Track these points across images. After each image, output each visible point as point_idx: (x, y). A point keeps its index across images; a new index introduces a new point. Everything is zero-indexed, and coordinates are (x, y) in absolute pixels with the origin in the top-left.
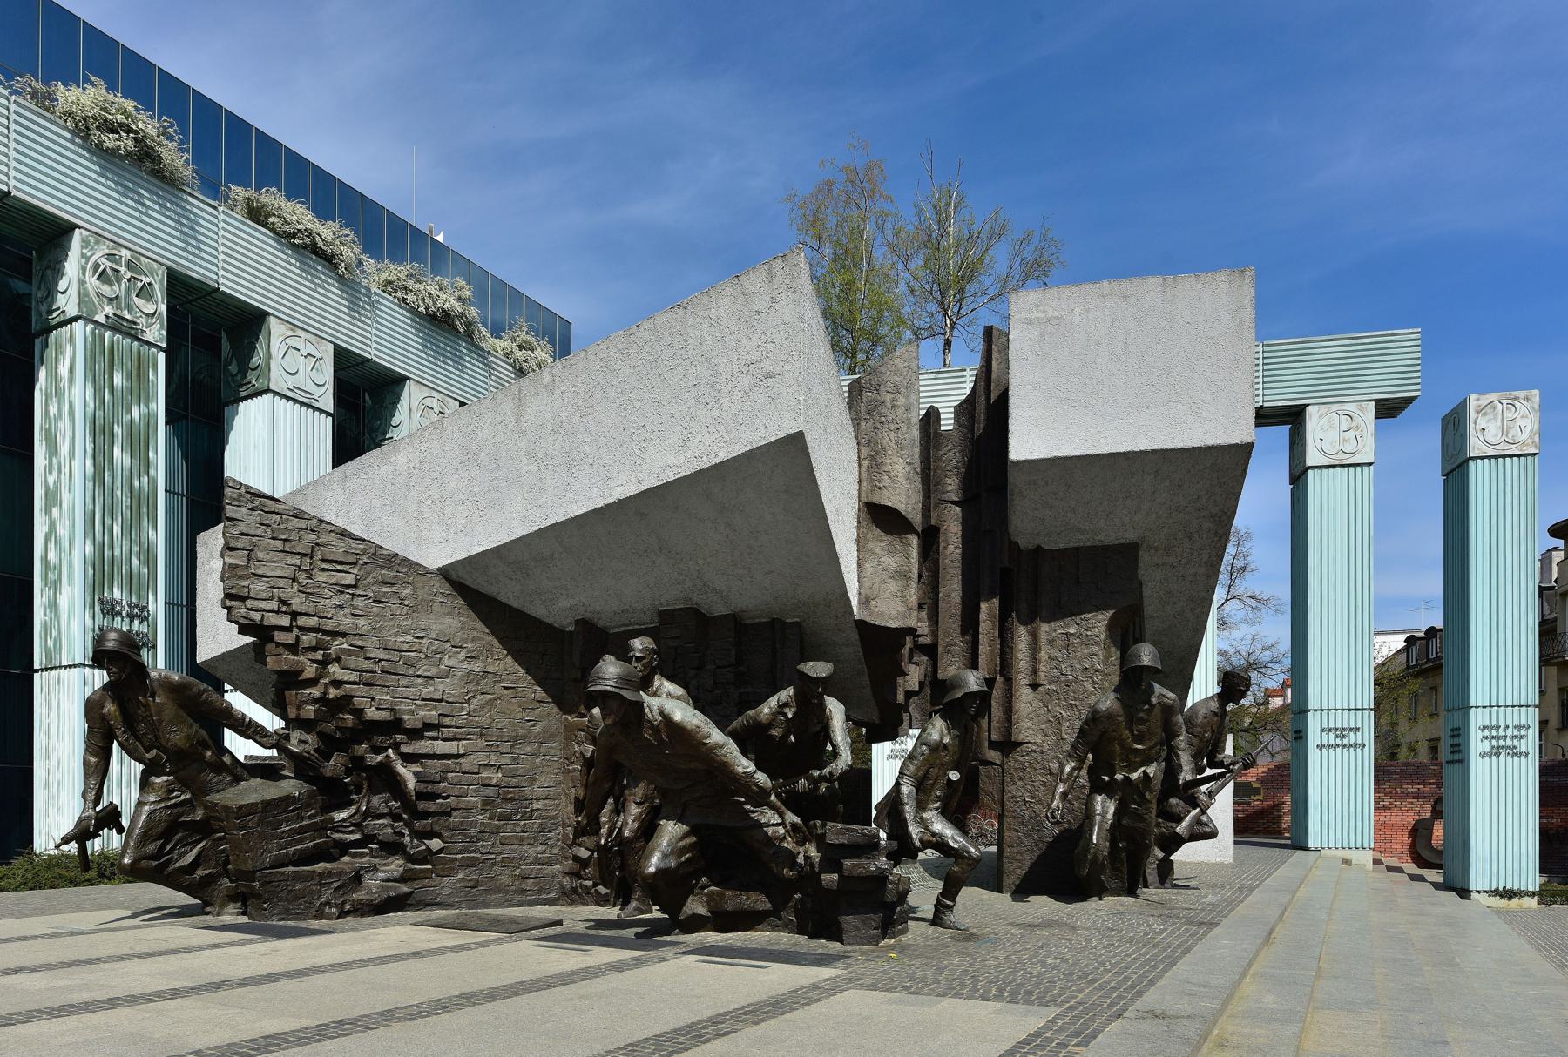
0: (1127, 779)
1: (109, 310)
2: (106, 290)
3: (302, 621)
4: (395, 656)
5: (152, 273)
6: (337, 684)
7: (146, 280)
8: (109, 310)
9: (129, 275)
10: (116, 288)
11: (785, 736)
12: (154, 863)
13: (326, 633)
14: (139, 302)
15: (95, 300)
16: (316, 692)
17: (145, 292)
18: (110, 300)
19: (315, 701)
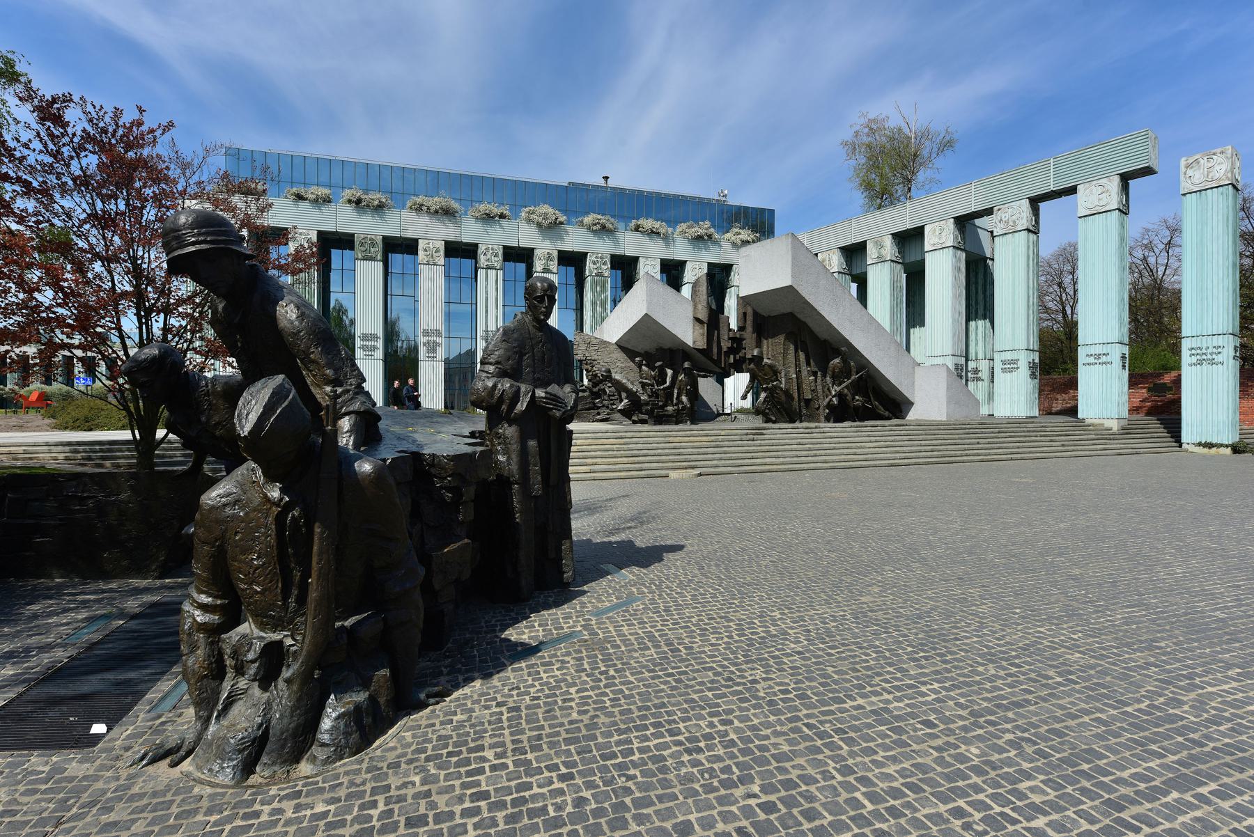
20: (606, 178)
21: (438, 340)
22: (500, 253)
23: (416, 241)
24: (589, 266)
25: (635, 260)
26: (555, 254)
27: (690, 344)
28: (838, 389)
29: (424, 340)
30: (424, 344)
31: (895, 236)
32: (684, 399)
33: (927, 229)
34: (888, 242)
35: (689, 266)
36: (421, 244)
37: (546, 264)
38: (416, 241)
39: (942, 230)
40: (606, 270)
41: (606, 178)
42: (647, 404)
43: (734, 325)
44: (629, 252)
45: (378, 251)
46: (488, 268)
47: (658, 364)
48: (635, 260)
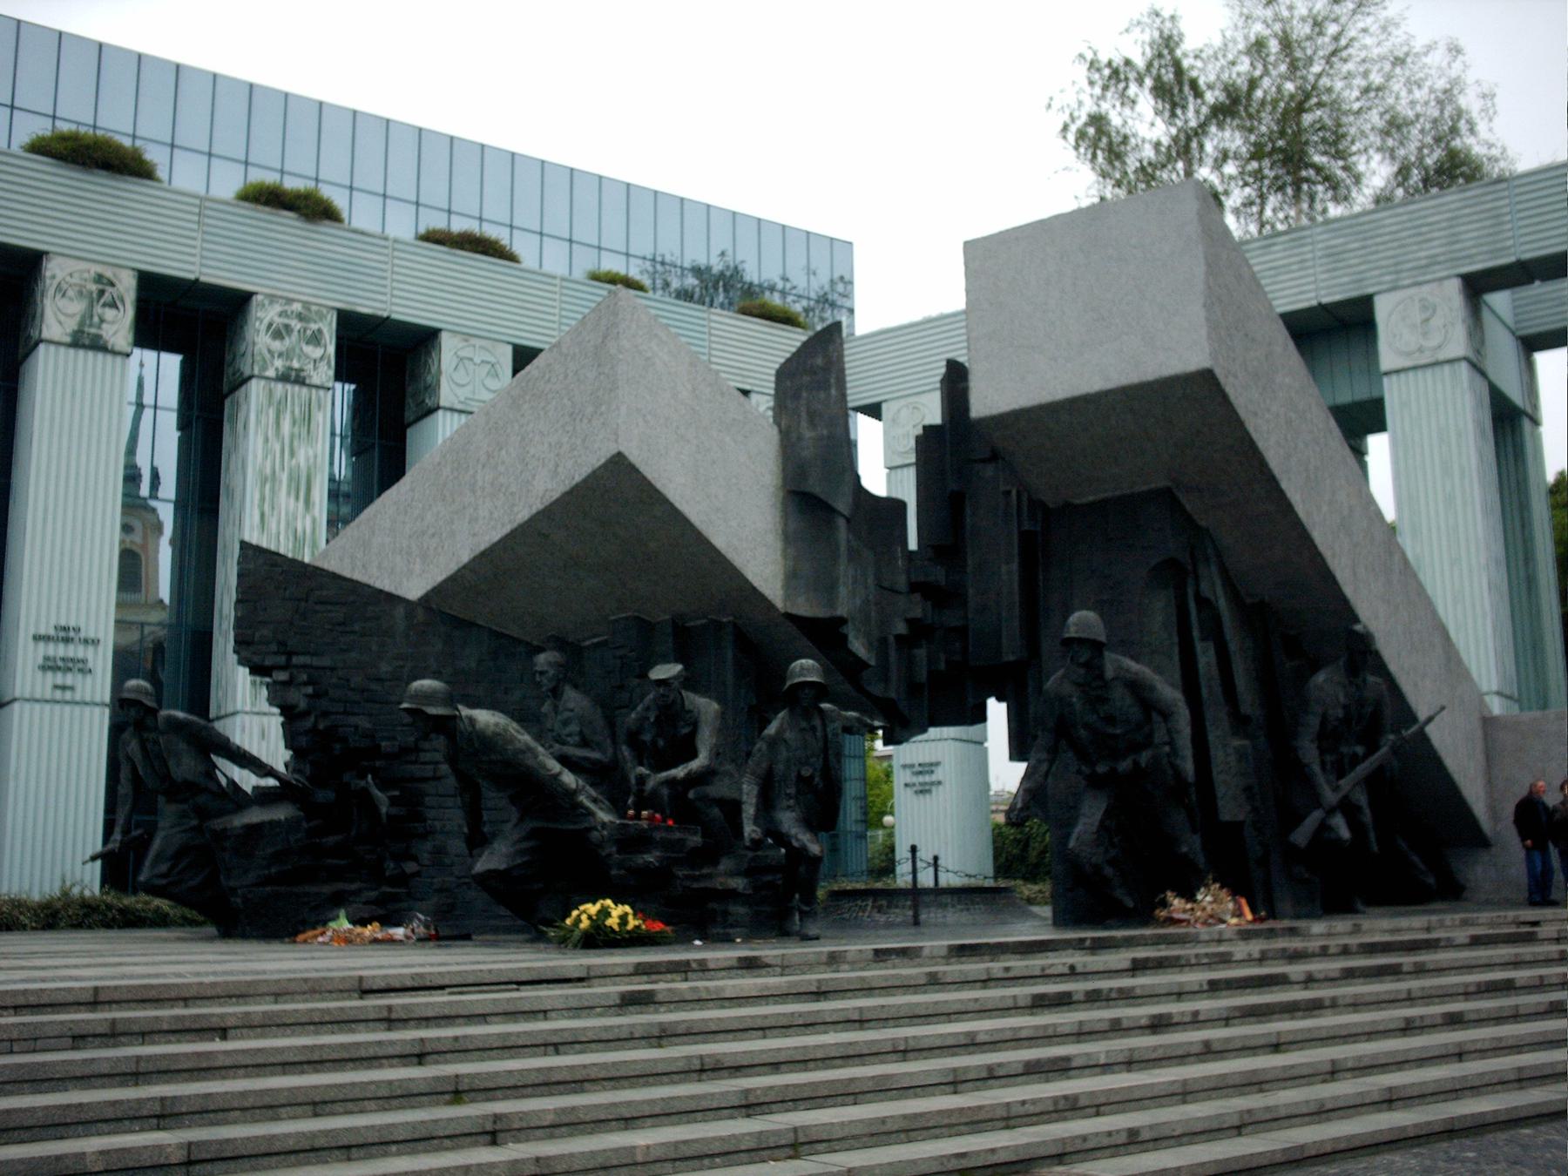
0: (1113, 770)
1: (279, 363)
2: (277, 345)
3: (295, 660)
4: (374, 686)
5: (322, 317)
6: (325, 714)
7: (314, 326)
8: (279, 363)
9: (299, 326)
10: (287, 341)
11: (654, 742)
12: (164, 882)
13: (317, 668)
14: (308, 349)
15: (268, 356)
16: (308, 723)
17: (316, 339)
18: (280, 355)
19: (306, 733)
25: (424, 339)
26: (127, 286)
27: (779, 603)
32: (788, 820)
33: (1383, 309)
39: (1428, 309)
40: (320, 360)
44: (408, 309)
47: (666, 671)
48: (424, 339)
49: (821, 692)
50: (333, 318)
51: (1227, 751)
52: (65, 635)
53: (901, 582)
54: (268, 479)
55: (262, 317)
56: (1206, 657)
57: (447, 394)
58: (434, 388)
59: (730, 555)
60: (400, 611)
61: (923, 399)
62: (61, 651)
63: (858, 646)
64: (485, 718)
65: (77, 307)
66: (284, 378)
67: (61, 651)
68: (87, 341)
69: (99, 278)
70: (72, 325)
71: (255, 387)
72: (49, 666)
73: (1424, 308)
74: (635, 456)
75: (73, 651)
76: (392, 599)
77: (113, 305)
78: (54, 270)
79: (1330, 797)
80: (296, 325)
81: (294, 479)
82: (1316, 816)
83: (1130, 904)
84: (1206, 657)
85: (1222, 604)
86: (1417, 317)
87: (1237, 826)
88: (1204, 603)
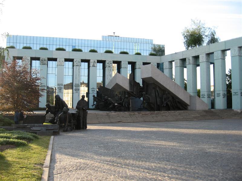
2: (108, 64)
17: (111, 63)
20: (114, 33)
21: (62, 87)
22: (80, 61)
23: (57, 58)
24: (107, 64)
26: (96, 61)
28: (165, 102)
29: (58, 87)
30: (58, 88)
31: (193, 57)
33: (200, 56)
34: (191, 58)
35: (137, 63)
36: (58, 60)
37: (93, 64)
38: (57, 58)
41: (114, 33)
42: (116, 106)
43: (141, 85)
45: (46, 62)
46: (77, 66)
49: (127, 97)
50: (112, 61)
51: (158, 100)
52: (93, 88)
53: (139, 88)
54: (108, 75)
55: (107, 62)
56: (157, 93)
57: (122, 67)
58: (121, 66)
59: (125, 88)
60: (109, 90)
61: (166, 63)
62: (93, 90)
63: (135, 93)
64: (109, 99)
65: (93, 64)
66: (108, 67)
67: (93, 90)
68: (94, 66)
69: (94, 61)
70: (92, 65)
71: (106, 68)
72: (92, 91)
73: (203, 56)
74: (118, 83)
75: (94, 90)
76: (109, 89)
77: (95, 63)
78: (91, 61)
79: (164, 103)
80: (109, 63)
81: (110, 75)
82: (163, 104)
83: (149, 110)
84: (157, 93)
85: (158, 90)
86: (202, 57)
87: (159, 105)
88: (157, 90)
